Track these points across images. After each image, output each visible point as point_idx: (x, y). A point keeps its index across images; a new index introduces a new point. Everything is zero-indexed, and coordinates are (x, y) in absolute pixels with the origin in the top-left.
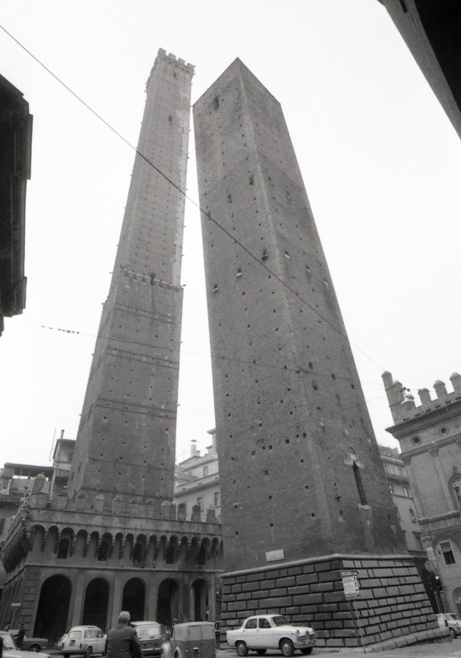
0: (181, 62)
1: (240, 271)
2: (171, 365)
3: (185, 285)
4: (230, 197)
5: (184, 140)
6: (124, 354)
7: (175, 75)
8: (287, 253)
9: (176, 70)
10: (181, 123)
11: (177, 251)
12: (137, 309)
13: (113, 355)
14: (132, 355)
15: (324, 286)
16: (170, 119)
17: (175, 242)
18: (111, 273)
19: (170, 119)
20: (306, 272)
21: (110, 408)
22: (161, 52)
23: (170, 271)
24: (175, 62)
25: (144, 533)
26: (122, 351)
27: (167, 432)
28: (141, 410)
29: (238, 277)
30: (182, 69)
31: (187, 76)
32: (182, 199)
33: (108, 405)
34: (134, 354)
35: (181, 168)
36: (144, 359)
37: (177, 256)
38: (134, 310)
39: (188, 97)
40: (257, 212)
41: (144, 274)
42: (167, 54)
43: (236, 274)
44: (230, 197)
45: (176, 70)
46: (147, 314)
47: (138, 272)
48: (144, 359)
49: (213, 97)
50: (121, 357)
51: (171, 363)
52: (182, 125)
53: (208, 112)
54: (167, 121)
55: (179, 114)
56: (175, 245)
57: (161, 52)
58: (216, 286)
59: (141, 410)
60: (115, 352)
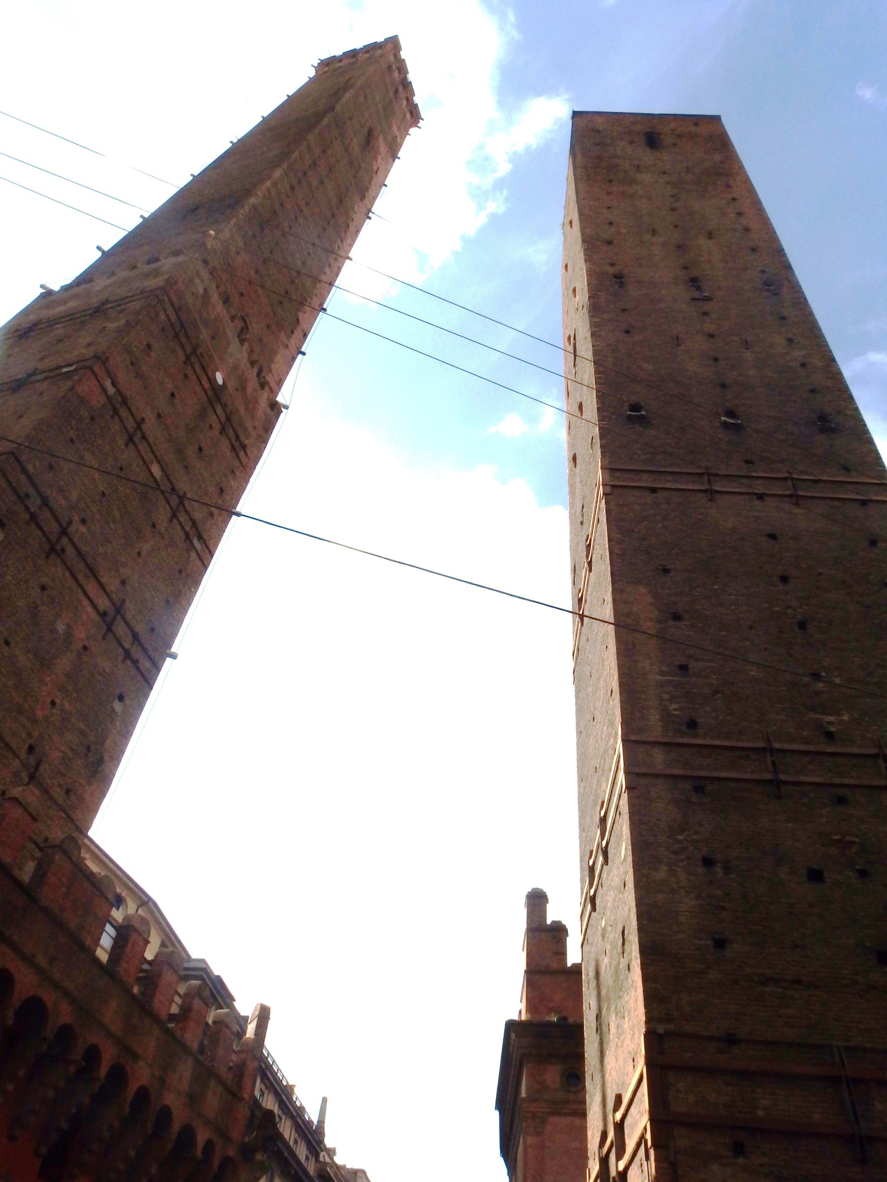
2: (195, 541)
3: (287, 407)
6: (123, 412)
9: (401, 89)
10: (379, 160)
12: (194, 351)
13: (104, 390)
14: (139, 433)
17: (301, 316)
18: (99, 248)
21: (27, 509)
25: (49, 997)
26: (125, 401)
27: (117, 706)
28: (91, 587)
29: (725, 424)
33: (27, 496)
34: (144, 437)
36: (156, 470)
38: (189, 350)
43: (717, 415)
45: (401, 89)
46: (207, 385)
48: (156, 470)
50: (116, 412)
51: (200, 537)
54: (366, 131)
56: (298, 319)
59: (91, 587)
60: (111, 390)
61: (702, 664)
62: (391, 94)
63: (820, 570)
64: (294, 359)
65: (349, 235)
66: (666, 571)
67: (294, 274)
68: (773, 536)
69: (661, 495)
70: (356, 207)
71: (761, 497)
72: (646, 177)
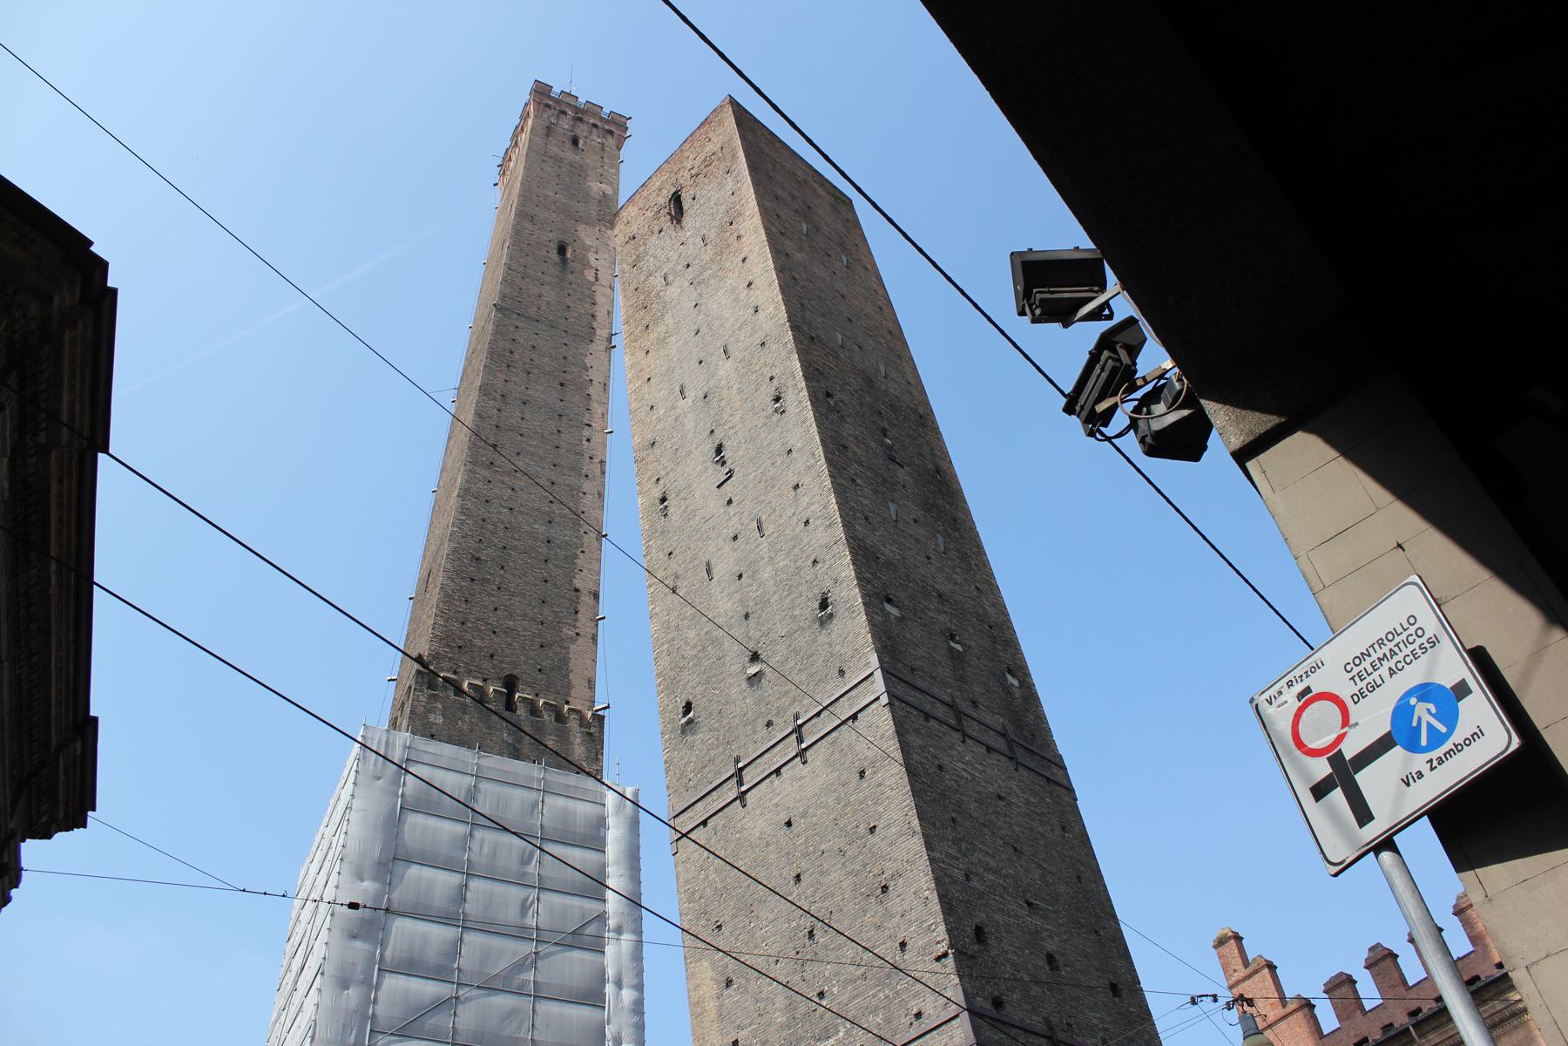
0: (593, 109)
1: (755, 657)
4: (719, 450)
5: (599, 299)
7: (575, 142)
8: (889, 601)
10: (591, 257)
11: (582, 609)
15: (1007, 689)
16: (562, 250)
17: (578, 583)
19: (562, 250)
20: (951, 649)
22: (541, 91)
23: (562, 667)
24: (576, 109)
30: (595, 126)
31: (611, 141)
32: (596, 460)
35: (592, 374)
37: (583, 617)
39: (609, 191)
40: (796, 487)
41: (485, 680)
42: (557, 90)
43: (744, 668)
44: (719, 450)
47: (469, 673)
49: (668, 192)
52: (594, 263)
53: (656, 229)
54: (554, 256)
55: (587, 235)
56: (577, 590)
57: (541, 91)
58: (688, 707)
61: (746, 1032)
62: (569, 155)
63: (823, 847)
64: (594, 638)
65: (594, 405)
66: (719, 927)
67: (544, 549)
68: (789, 824)
69: (711, 823)
70: (588, 361)
71: (778, 771)
72: (673, 292)
